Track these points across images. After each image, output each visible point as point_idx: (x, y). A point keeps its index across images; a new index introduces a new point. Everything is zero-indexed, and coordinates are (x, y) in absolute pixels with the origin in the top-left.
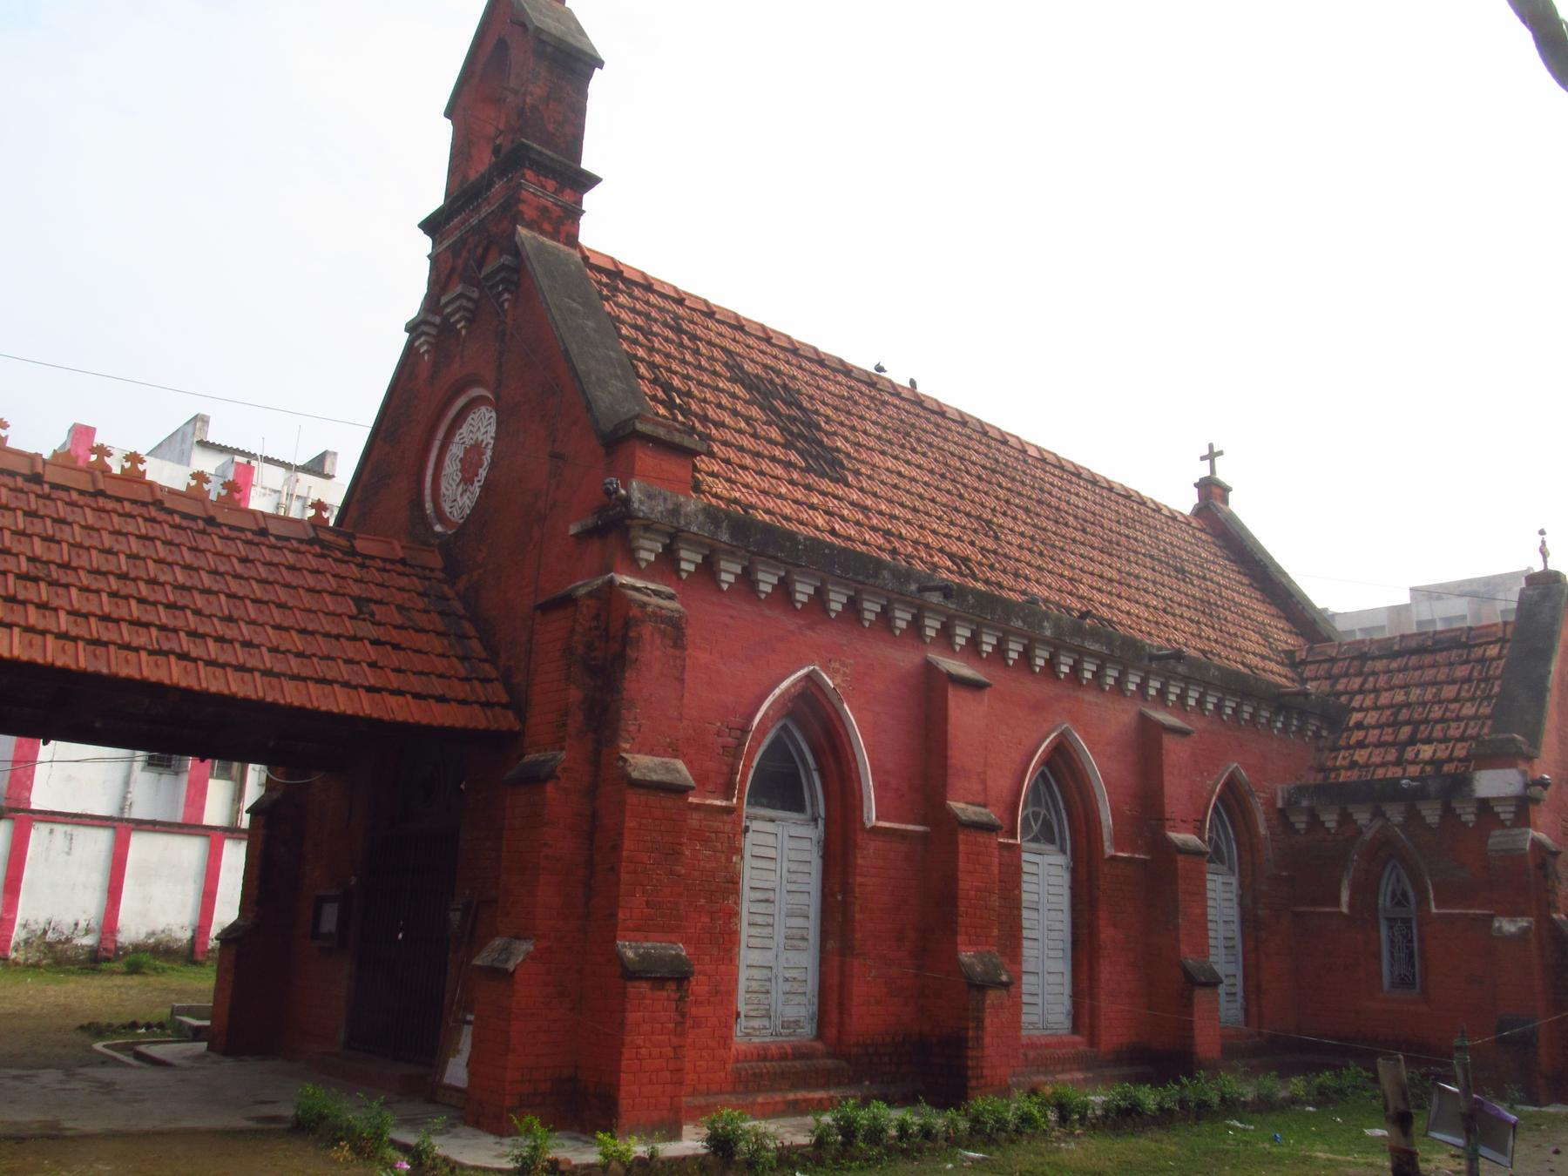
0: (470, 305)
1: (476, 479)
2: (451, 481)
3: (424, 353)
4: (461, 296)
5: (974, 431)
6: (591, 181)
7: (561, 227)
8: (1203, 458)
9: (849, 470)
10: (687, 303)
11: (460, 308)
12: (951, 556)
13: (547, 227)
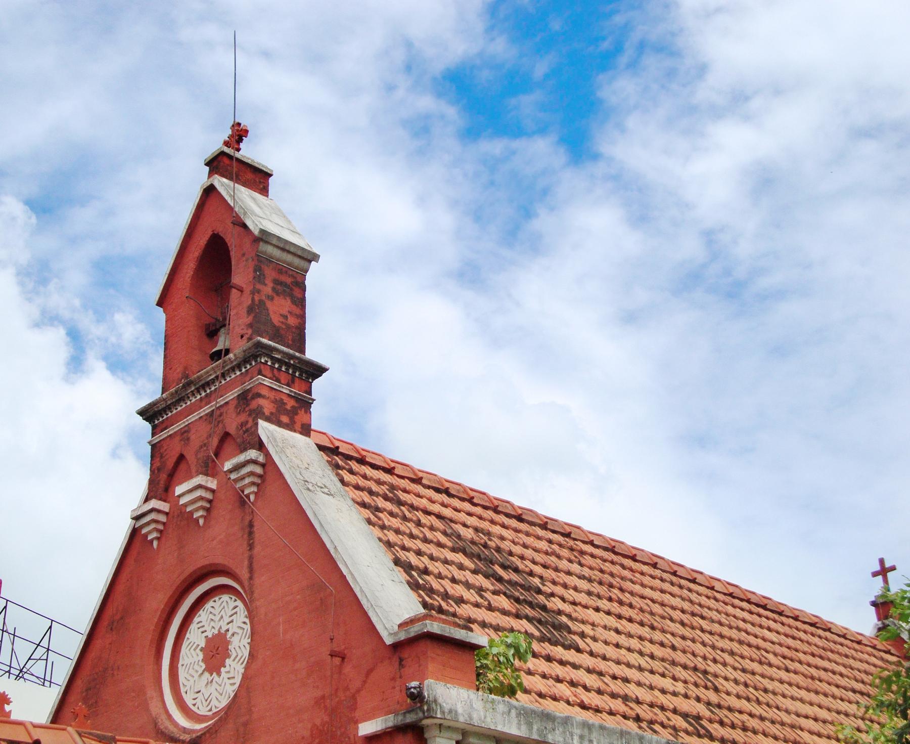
0: (209, 496)
2: (191, 671)
5: (664, 571)
6: (317, 371)
7: (296, 417)
8: (875, 574)
9: (575, 633)
10: (424, 481)
12: (685, 716)
13: (285, 419)
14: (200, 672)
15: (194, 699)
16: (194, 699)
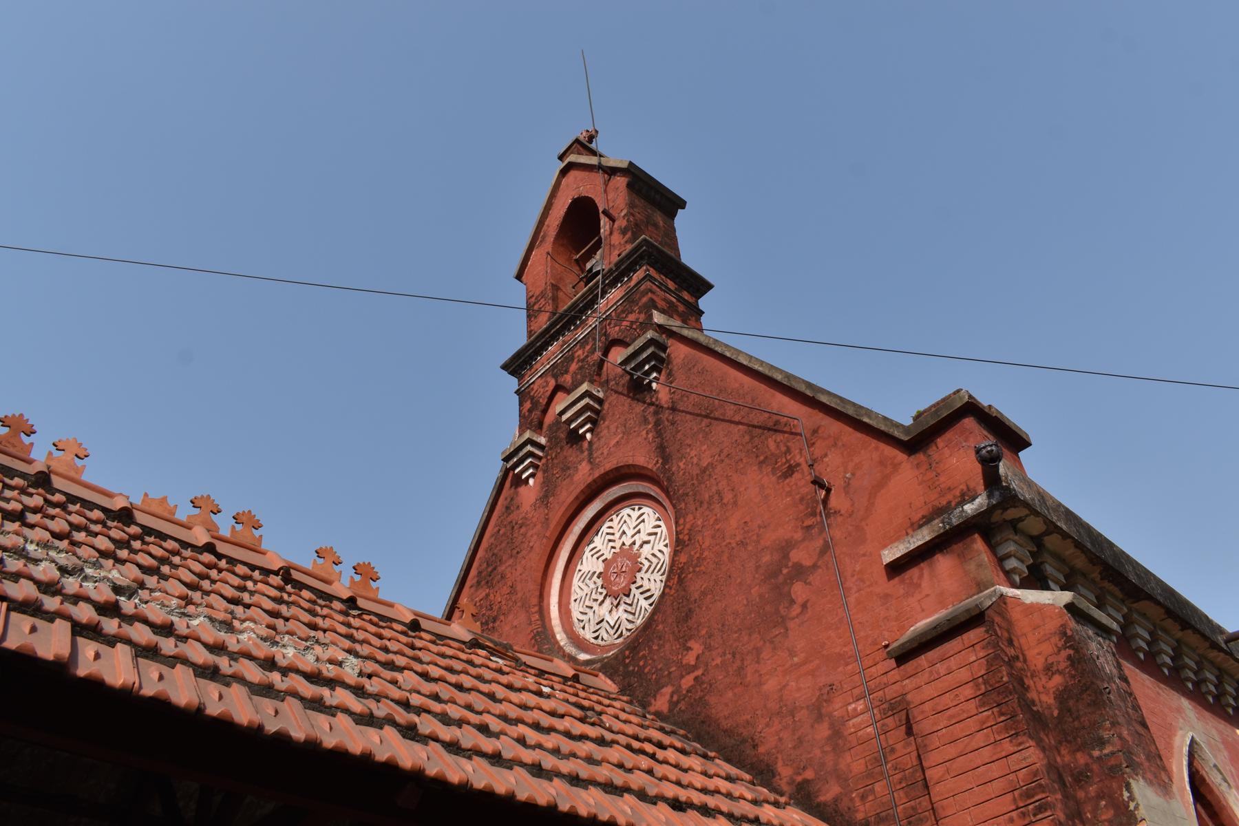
1: (633, 587)
3: (527, 478)
4: (587, 394)
11: (587, 408)
14: (601, 598)
15: (594, 632)
16: (594, 632)
